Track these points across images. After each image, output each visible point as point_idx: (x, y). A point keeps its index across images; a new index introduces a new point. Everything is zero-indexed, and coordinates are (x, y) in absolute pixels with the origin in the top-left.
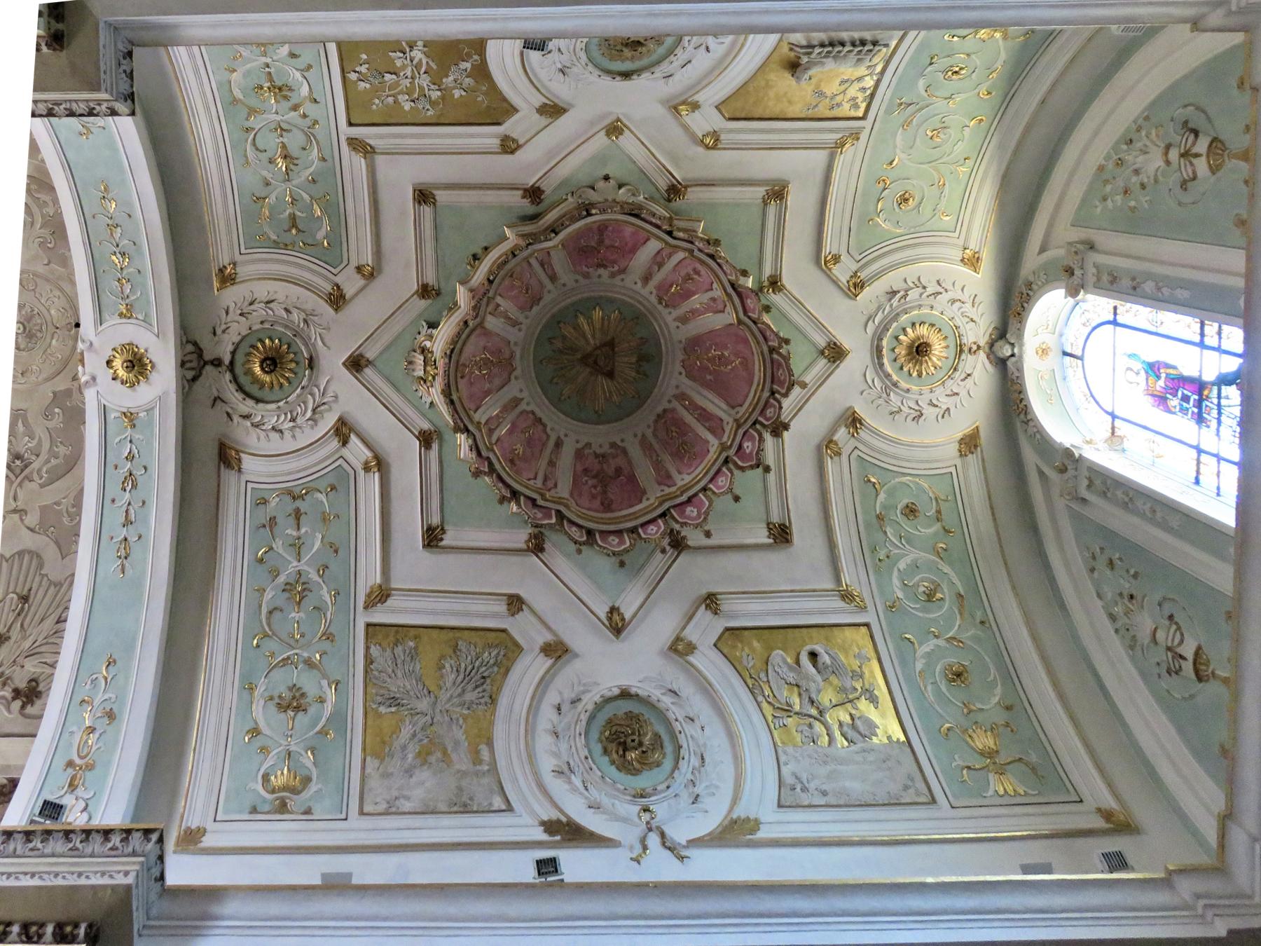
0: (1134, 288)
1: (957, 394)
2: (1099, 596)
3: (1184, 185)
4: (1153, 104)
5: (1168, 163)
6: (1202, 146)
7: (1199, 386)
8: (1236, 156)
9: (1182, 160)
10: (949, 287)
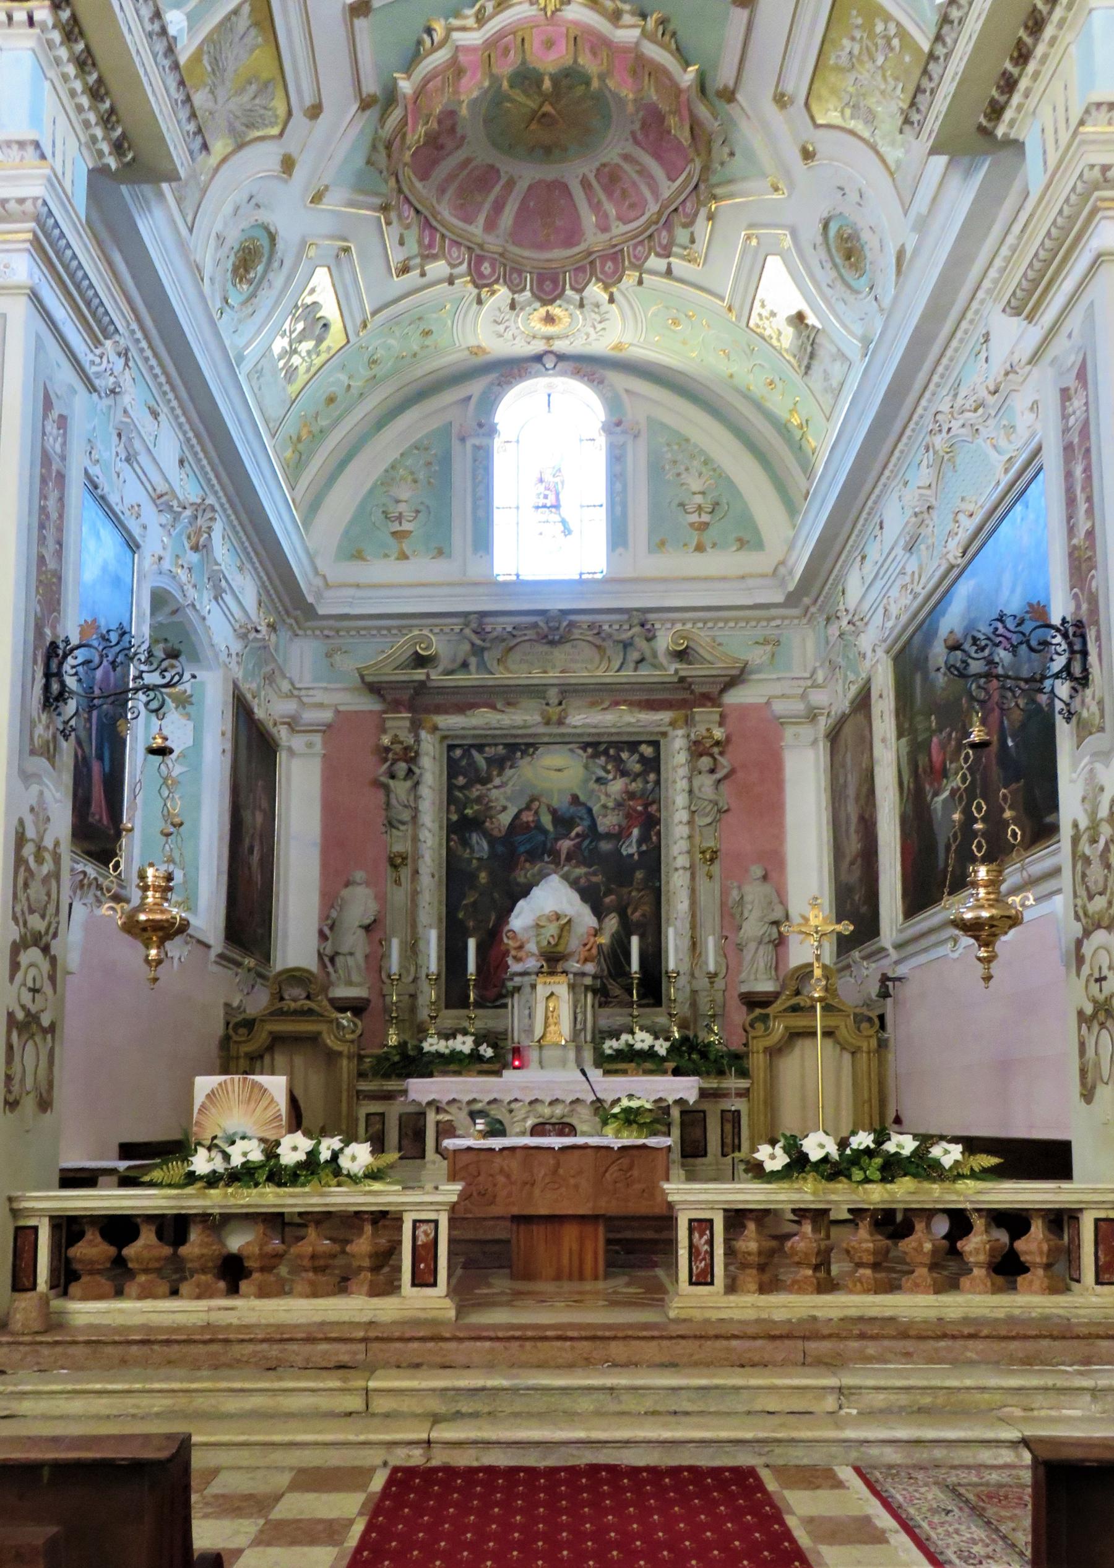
7: (556, 506)
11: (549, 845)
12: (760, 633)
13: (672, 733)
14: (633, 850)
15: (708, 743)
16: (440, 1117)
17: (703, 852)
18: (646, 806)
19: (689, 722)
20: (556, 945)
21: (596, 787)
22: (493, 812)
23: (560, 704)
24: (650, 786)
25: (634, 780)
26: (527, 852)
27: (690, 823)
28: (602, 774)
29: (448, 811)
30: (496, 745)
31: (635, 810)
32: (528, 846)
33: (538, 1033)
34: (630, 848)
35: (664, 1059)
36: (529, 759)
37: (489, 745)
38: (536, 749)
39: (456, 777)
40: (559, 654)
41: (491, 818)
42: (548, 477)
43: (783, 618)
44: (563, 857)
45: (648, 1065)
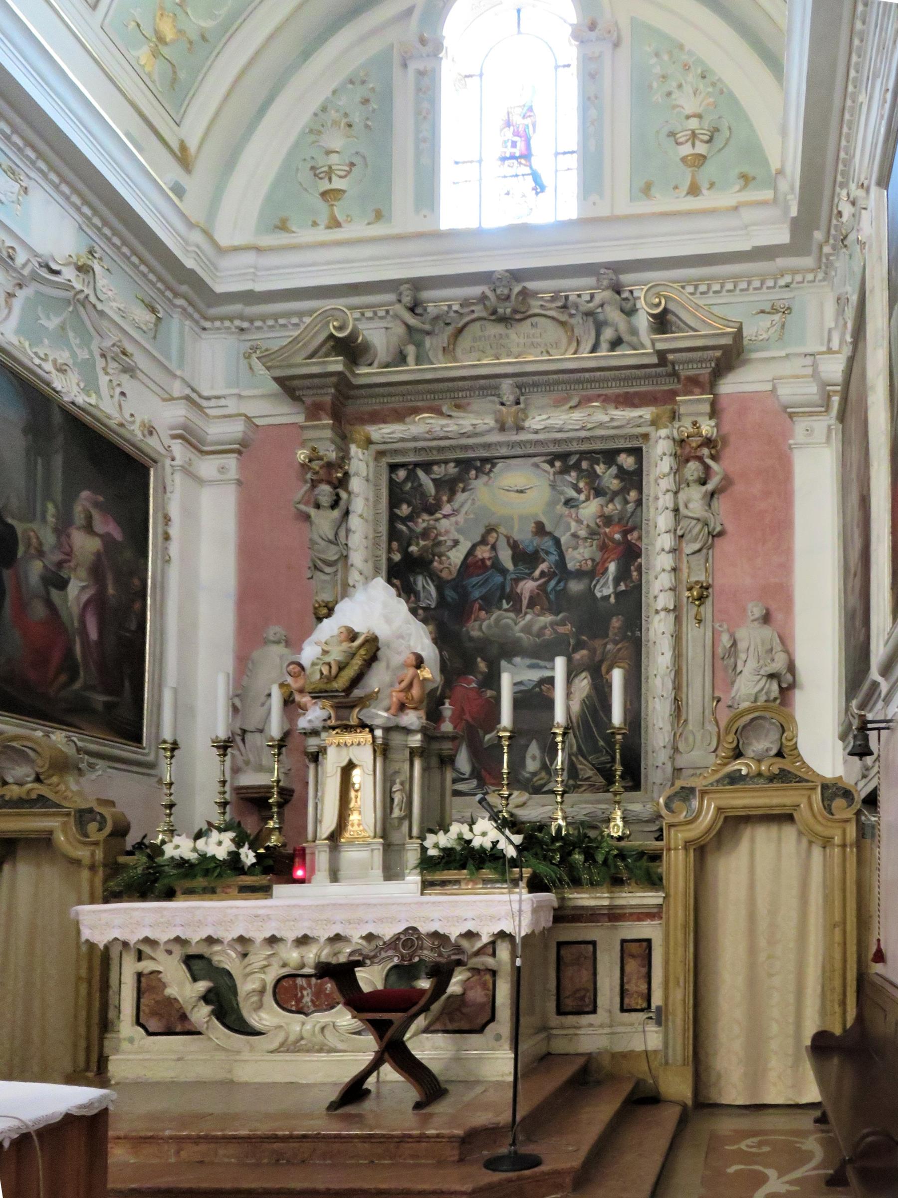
2: (334, 92)
3: (672, 134)
5: (688, 117)
6: (701, 148)
7: (526, 156)
9: (690, 132)
11: (508, 590)
14: (609, 590)
21: (566, 511)
23: (518, 403)
24: (630, 507)
25: (611, 500)
26: (481, 598)
28: (574, 494)
29: (390, 550)
30: (446, 462)
31: (612, 540)
32: (484, 590)
34: (605, 589)
36: (484, 478)
38: (494, 465)
39: (398, 507)
41: (440, 555)
42: (517, 119)
44: (525, 602)
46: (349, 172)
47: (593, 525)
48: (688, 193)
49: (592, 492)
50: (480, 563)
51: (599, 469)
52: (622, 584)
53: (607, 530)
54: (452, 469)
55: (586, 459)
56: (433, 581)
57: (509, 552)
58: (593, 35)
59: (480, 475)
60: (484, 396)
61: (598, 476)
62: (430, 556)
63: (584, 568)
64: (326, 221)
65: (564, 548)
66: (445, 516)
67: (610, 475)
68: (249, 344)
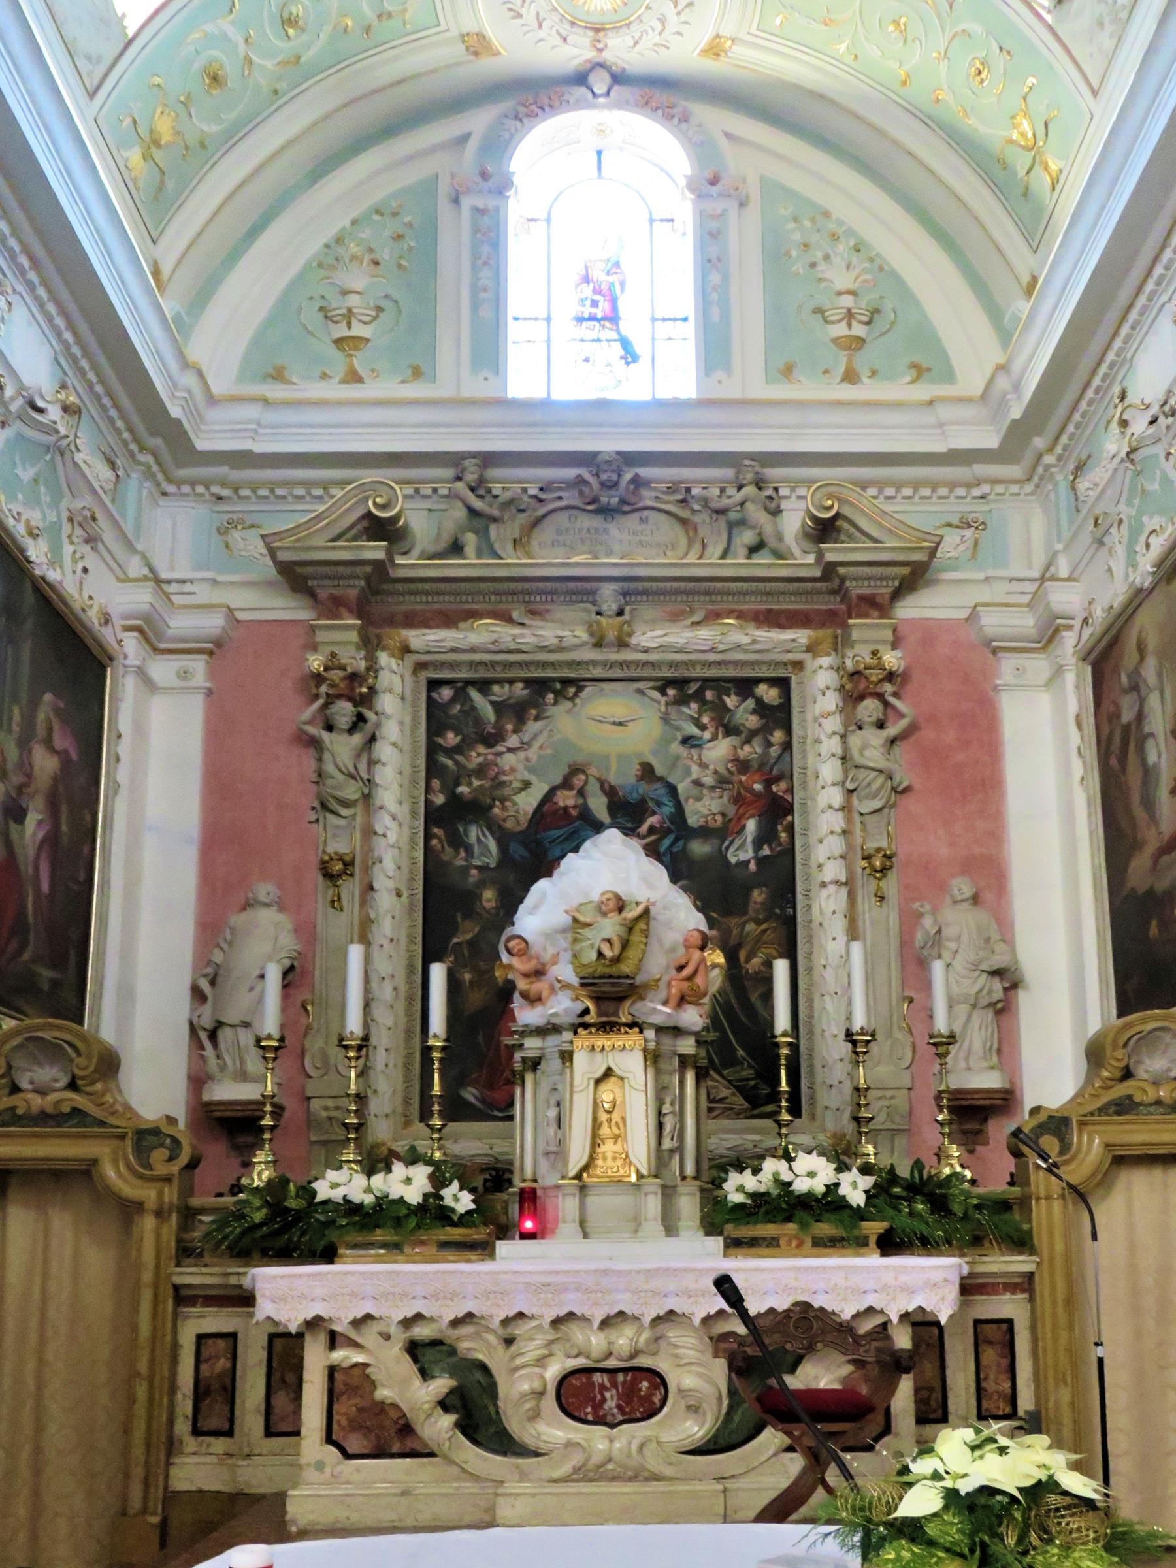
0: (709, 261)
1: (540, 26)
3: (819, 311)
4: (895, 276)
5: (839, 294)
6: (859, 330)
8: (849, 362)
9: (844, 311)
10: (683, 18)
12: (953, 509)
13: (811, 663)
14: (747, 854)
15: (875, 675)
16: (340, 1355)
17: (867, 857)
18: (768, 783)
19: (840, 644)
20: (617, 960)
21: (683, 751)
22: (506, 791)
24: (774, 751)
25: (748, 741)
27: (846, 808)
28: (695, 731)
30: (511, 682)
31: (750, 790)
33: (577, 1156)
34: (742, 852)
35: (860, 1215)
36: (568, 704)
37: (499, 682)
38: (580, 689)
40: (620, 532)
43: (995, 481)
45: (825, 1229)
46: (375, 318)
47: (722, 770)
48: (843, 380)
49: (721, 730)
50: (561, 812)
51: (731, 701)
52: (765, 847)
53: (743, 778)
54: (519, 690)
55: (711, 688)
56: (493, 834)
57: (604, 800)
58: (714, 190)
59: (561, 700)
60: (572, 602)
61: (729, 710)
62: (489, 801)
63: (711, 825)
64: (342, 375)
65: (682, 798)
66: (510, 750)
67: (746, 711)
68: (227, 517)
